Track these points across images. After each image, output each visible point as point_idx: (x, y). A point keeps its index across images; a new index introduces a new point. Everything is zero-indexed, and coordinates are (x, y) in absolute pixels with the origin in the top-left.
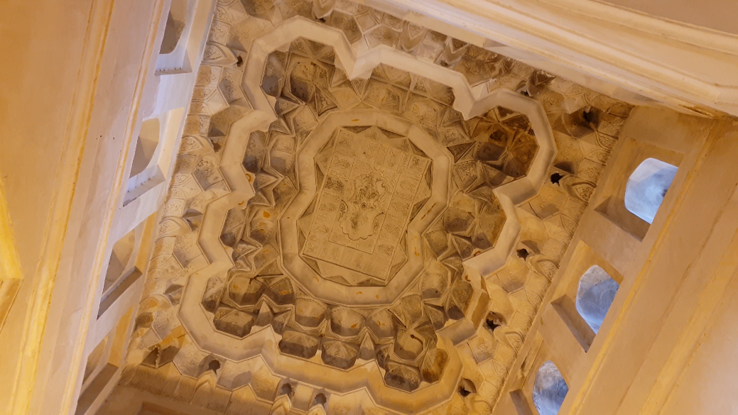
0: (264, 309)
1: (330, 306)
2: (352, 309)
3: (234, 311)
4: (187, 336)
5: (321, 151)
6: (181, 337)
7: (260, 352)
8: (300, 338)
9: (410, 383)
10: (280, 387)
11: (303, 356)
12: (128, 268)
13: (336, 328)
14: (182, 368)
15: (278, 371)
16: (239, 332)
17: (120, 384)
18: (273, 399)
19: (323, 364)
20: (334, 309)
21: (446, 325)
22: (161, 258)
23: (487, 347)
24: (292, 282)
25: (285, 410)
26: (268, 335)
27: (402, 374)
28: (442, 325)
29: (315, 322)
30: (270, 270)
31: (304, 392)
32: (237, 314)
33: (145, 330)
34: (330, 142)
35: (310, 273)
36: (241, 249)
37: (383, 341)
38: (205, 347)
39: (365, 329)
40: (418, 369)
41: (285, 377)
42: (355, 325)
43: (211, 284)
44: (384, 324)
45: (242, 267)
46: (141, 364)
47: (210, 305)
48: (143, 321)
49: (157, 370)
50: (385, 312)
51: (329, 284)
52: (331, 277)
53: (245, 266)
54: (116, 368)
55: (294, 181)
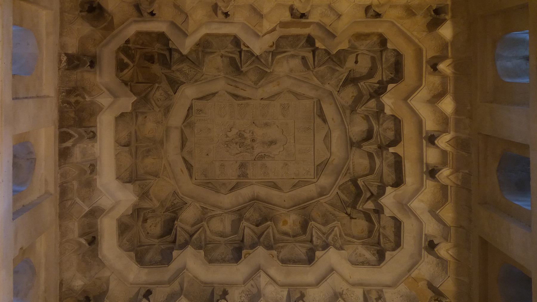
5: (218, 192)
13: (369, 136)
34: (208, 184)
55: (248, 207)
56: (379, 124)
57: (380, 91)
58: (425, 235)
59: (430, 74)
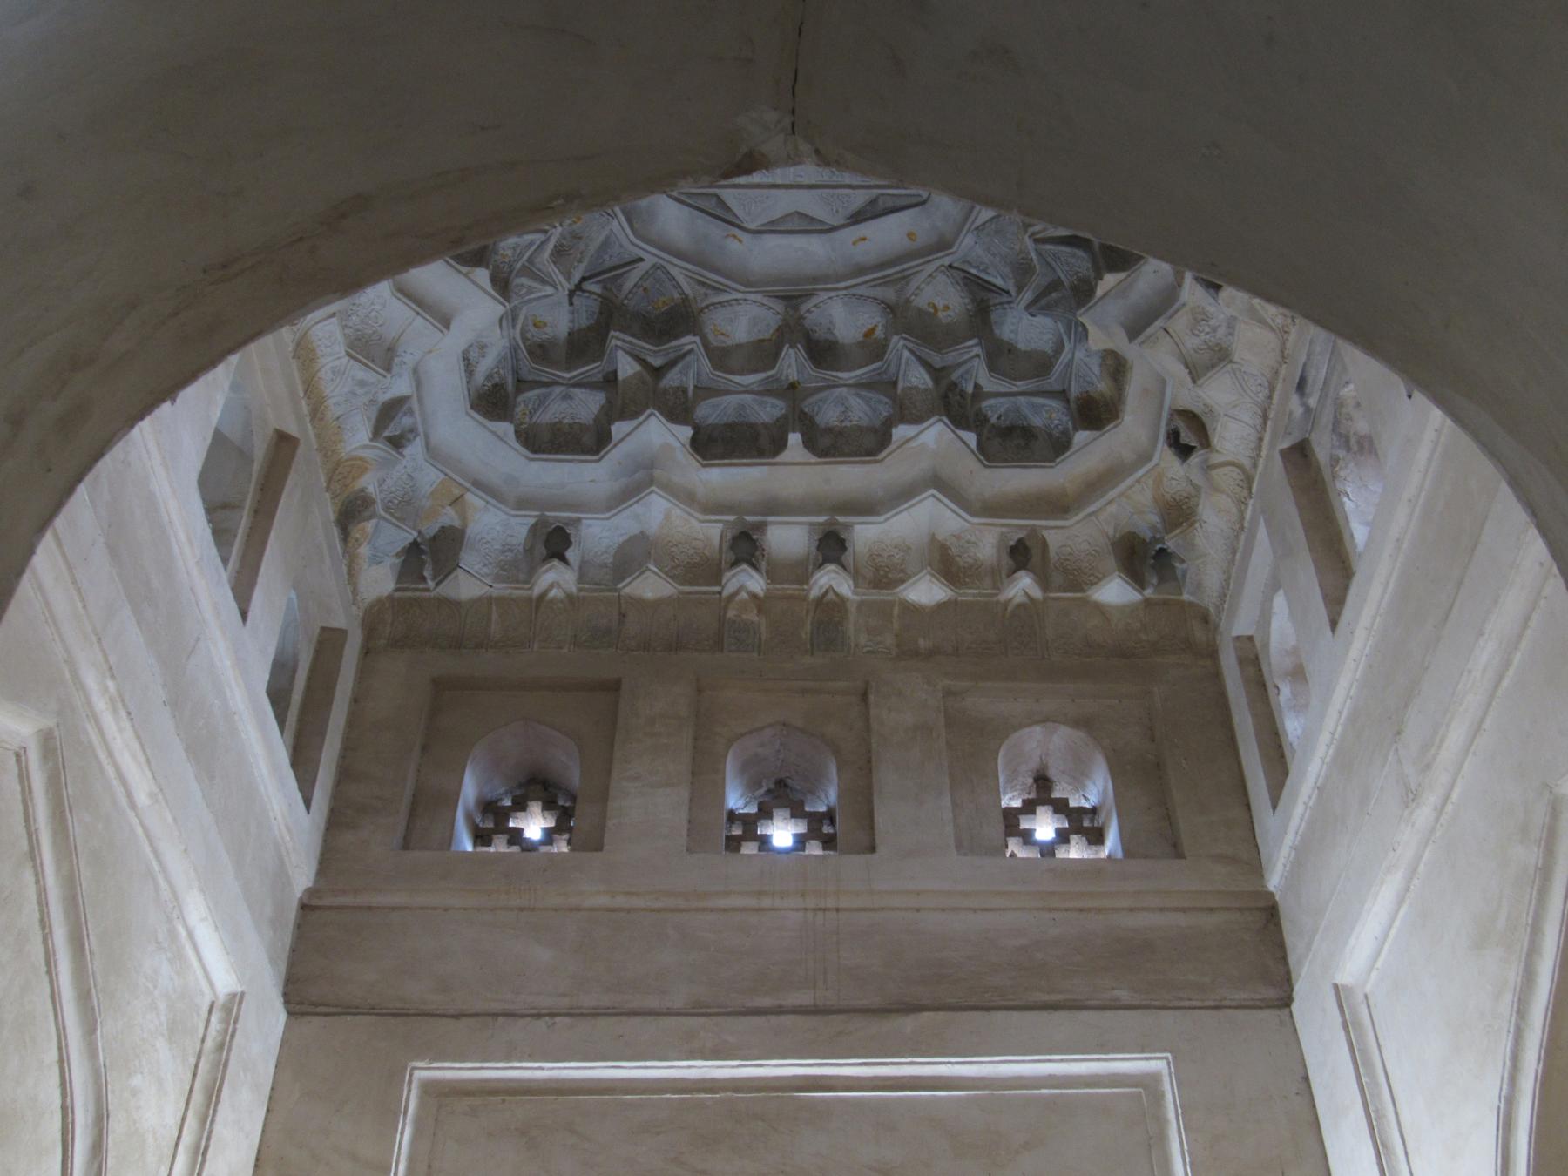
0: (627, 368)
1: (792, 300)
2: (853, 291)
3: (558, 390)
4: (469, 497)
6: (457, 501)
7: (651, 481)
8: (742, 407)
9: (1050, 435)
10: (725, 546)
11: (761, 453)
12: (260, 450)
13: (823, 352)
14: (485, 570)
15: (713, 508)
16: (588, 439)
17: (367, 652)
18: (716, 578)
19: (814, 459)
20: (804, 308)
21: (1099, 292)
22: (325, 374)
23: (1214, 330)
24: (675, 271)
25: (754, 596)
26: (656, 434)
27: (1026, 418)
28: (1091, 291)
29: (763, 353)
30: (607, 257)
31: (788, 538)
32: (567, 397)
33: (370, 526)
35: (715, 230)
36: (509, 253)
37: (951, 357)
38: (522, 504)
39: (897, 342)
40: (1063, 395)
41: (732, 518)
42: (872, 330)
43: (473, 355)
44: (947, 308)
45: (530, 290)
46: (397, 590)
47: (492, 401)
48: (351, 513)
49: (434, 589)
50: (941, 278)
51: (771, 241)
52: (772, 223)
53: (535, 285)
54: (342, 633)
56: (859, 385)
57: (956, 406)
58: (579, 520)
59: (1003, 536)
